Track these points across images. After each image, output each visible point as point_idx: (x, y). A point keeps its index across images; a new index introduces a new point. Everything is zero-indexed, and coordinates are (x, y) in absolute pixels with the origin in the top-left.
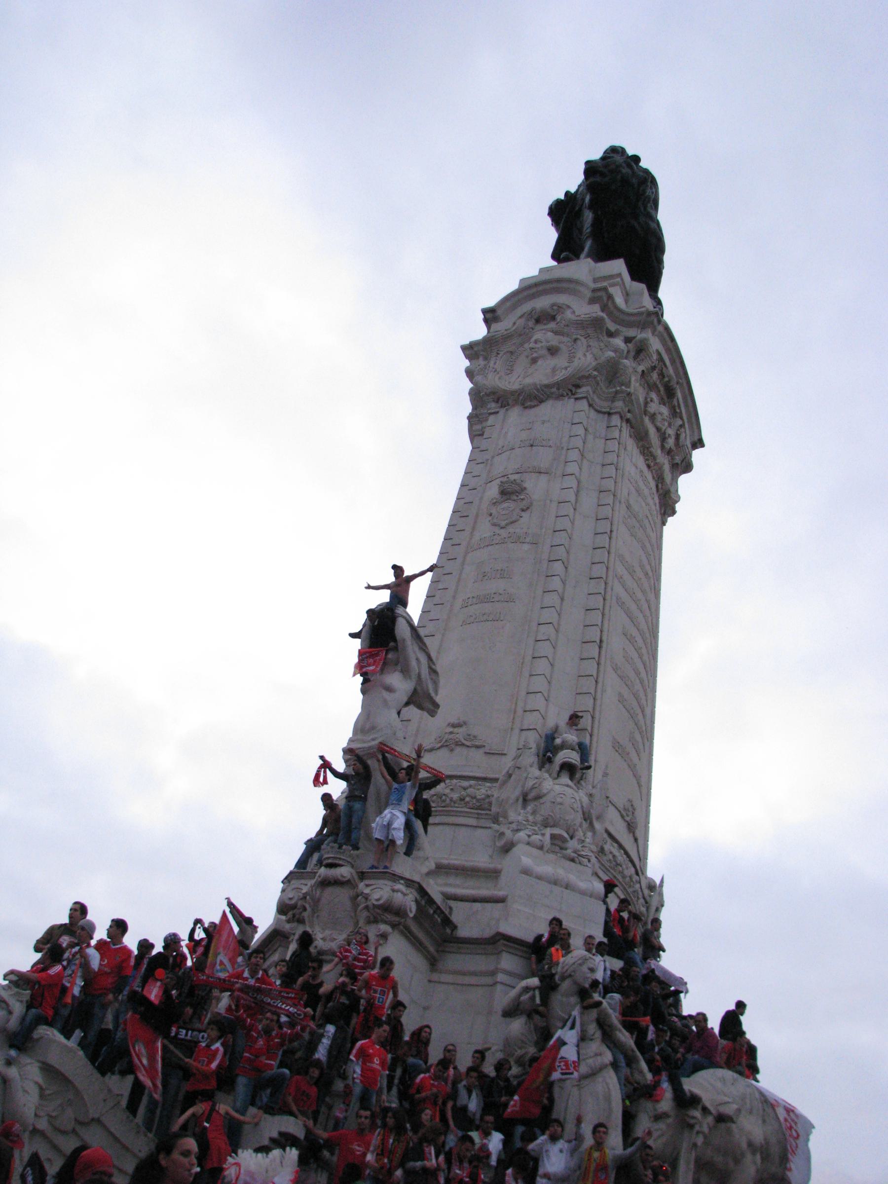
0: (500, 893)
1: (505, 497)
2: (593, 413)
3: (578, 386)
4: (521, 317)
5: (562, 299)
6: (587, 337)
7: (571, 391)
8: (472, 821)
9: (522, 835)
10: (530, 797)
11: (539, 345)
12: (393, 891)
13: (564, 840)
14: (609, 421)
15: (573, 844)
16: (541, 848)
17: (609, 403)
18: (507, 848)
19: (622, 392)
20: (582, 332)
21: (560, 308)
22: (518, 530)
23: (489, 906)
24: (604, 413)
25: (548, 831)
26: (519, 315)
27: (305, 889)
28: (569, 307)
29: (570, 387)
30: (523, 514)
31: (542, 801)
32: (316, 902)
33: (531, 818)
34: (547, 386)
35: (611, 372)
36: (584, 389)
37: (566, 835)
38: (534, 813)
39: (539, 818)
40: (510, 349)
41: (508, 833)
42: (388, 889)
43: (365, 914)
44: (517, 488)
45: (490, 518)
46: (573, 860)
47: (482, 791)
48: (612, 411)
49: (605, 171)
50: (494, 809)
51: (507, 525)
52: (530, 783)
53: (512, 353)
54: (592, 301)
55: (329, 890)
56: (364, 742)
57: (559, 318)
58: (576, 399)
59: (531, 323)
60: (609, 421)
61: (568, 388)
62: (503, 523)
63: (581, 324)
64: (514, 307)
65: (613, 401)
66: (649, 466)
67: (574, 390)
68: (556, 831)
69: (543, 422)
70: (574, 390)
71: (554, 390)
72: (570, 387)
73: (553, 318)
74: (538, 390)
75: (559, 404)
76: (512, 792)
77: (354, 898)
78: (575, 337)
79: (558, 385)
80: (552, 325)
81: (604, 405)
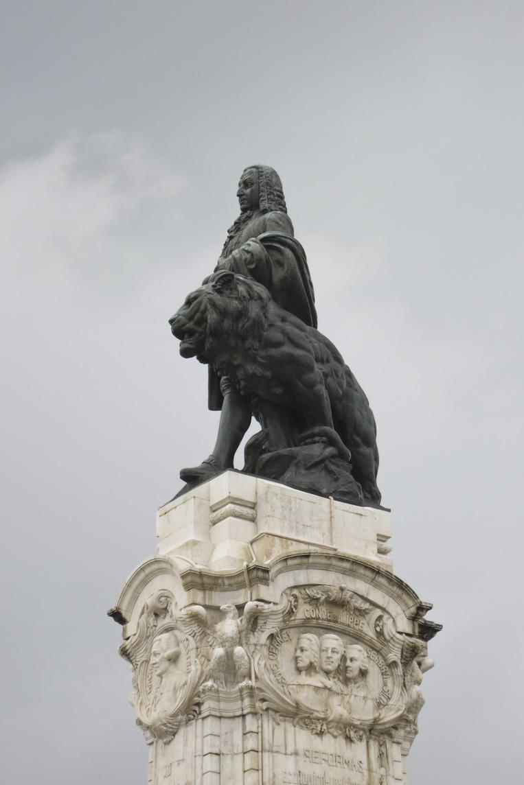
2: (226, 724)
3: (199, 704)
4: (142, 613)
7: (195, 711)
24: (238, 716)
34: (175, 715)
35: (229, 669)
36: (204, 707)
40: (144, 659)
49: (190, 325)
58: (203, 718)
59: (152, 620)
60: (244, 727)
61: (191, 709)
66: (321, 734)
69: (179, 762)
71: (180, 717)
75: (191, 729)
81: (235, 707)
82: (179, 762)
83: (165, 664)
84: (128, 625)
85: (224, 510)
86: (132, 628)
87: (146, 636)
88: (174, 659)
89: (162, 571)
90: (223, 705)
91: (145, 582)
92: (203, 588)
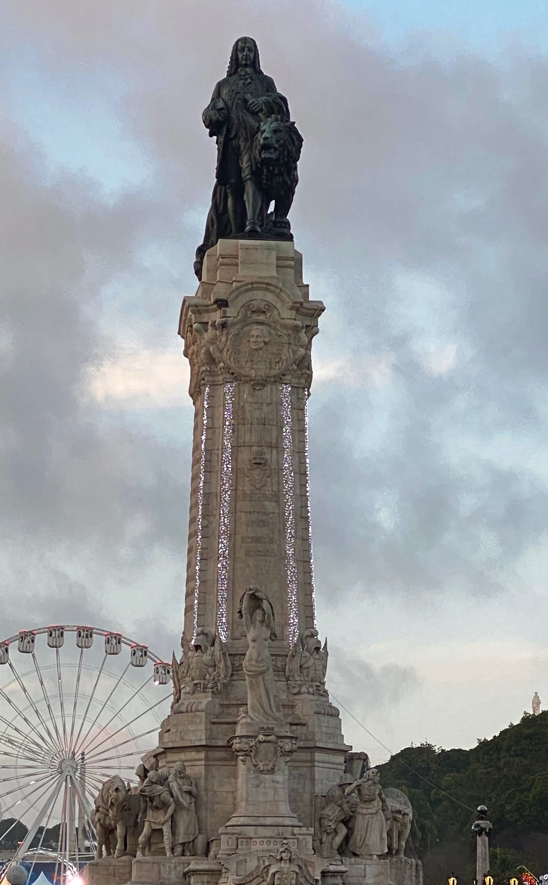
0: (304, 722)
1: (255, 466)
3: (284, 375)
5: (270, 297)
6: (288, 336)
7: (281, 378)
9: (304, 689)
10: (303, 667)
11: (259, 340)
12: (292, 744)
14: (298, 394)
16: (313, 694)
17: (297, 380)
19: (306, 373)
20: (284, 331)
21: (270, 307)
22: (267, 492)
23: (299, 727)
26: (241, 305)
27: (251, 744)
28: (275, 307)
29: (281, 376)
30: (269, 480)
31: (310, 669)
32: (257, 748)
33: (306, 679)
36: (288, 377)
39: (310, 678)
42: (290, 744)
43: (281, 754)
44: (263, 462)
45: (247, 479)
46: (322, 695)
48: (300, 386)
50: (287, 674)
51: (261, 487)
52: (304, 660)
53: (237, 335)
54: (292, 308)
55: (264, 744)
56: (259, 667)
57: (268, 314)
60: (298, 394)
62: (258, 486)
63: (285, 326)
64: (237, 296)
65: (299, 378)
69: (268, 404)
70: (283, 378)
71: (272, 379)
72: (281, 376)
73: (264, 312)
74: (263, 380)
76: (295, 665)
77: (275, 749)
78: (279, 333)
79: (274, 376)
80: (262, 318)
82: (268, 404)
83: (262, 344)
84: (228, 309)
86: (231, 311)
87: (245, 322)
88: (266, 343)
89: (266, 290)
90: (292, 379)
91: (248, 290)
92: (297, 310)
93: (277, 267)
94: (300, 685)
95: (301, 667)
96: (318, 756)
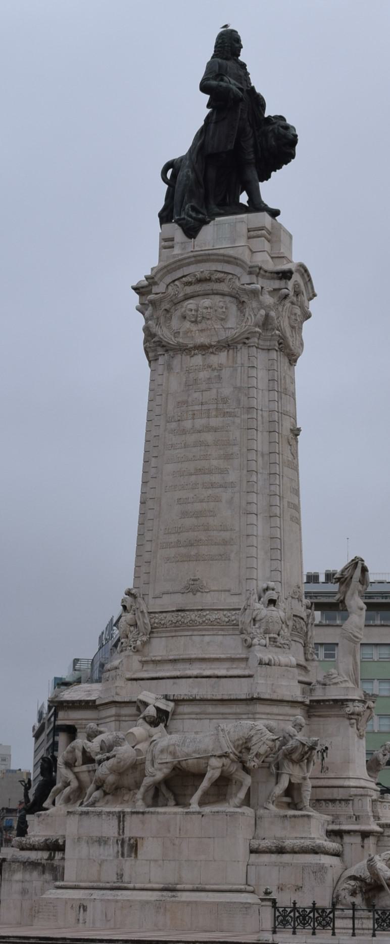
0: (251, 673)
3: (248, 338)
8: (231, 632)
9: (255, 641)
13: (275, 638)
15: (280, 639)
18: (250, 646)
25: (267, 636)
35: (266, 324)
37: (276, 636)
38: (259, 627)
39: (262, 630)
41: (249, 639)
47: (233, 616)
54: (250, 273)
67: (247, 341)
68: (272, 635)
70: (247, 341)
85: (260, 232)
93: (249, 238)
94: (253, 639)
95: (254, 620)
96: (260, 708)
